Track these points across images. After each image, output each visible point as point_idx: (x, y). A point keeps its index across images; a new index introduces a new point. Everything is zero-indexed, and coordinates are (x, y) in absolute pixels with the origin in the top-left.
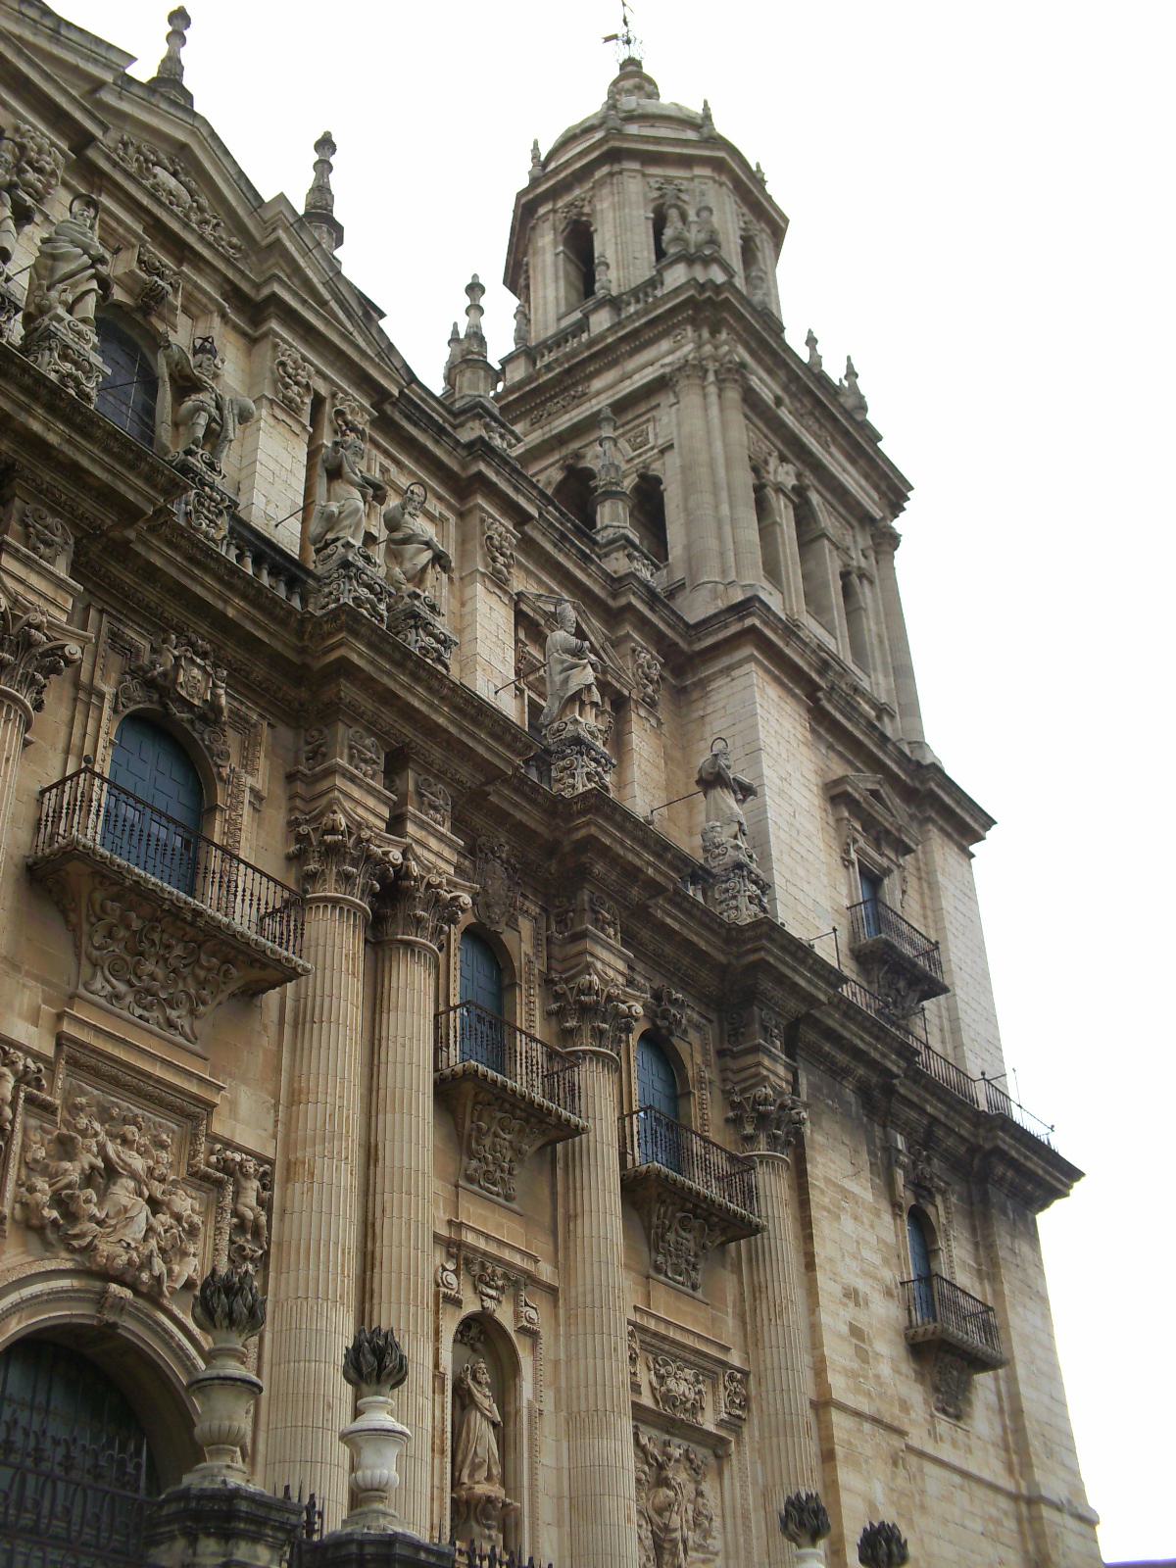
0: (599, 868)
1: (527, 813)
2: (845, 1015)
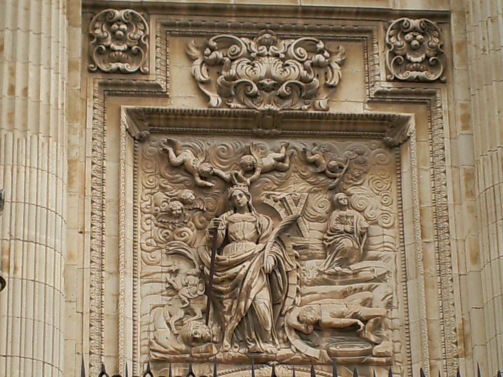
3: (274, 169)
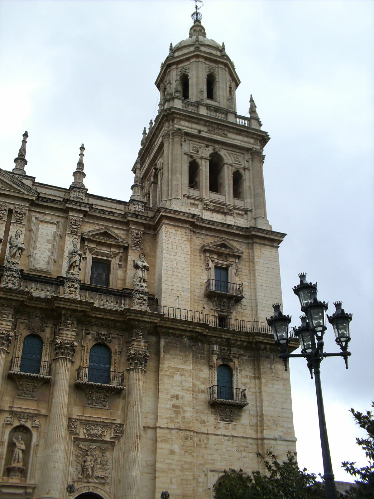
0: (64, 312)
1: (39, 304)
2: (173, 322)
3: (95, 449)
